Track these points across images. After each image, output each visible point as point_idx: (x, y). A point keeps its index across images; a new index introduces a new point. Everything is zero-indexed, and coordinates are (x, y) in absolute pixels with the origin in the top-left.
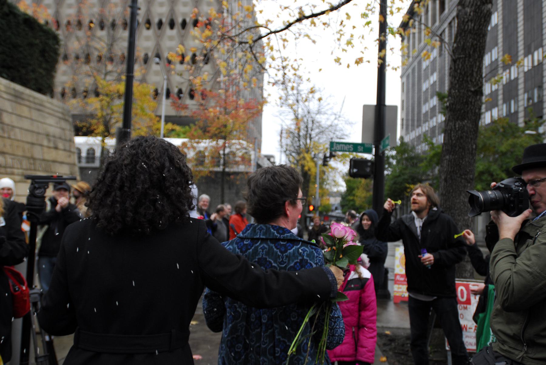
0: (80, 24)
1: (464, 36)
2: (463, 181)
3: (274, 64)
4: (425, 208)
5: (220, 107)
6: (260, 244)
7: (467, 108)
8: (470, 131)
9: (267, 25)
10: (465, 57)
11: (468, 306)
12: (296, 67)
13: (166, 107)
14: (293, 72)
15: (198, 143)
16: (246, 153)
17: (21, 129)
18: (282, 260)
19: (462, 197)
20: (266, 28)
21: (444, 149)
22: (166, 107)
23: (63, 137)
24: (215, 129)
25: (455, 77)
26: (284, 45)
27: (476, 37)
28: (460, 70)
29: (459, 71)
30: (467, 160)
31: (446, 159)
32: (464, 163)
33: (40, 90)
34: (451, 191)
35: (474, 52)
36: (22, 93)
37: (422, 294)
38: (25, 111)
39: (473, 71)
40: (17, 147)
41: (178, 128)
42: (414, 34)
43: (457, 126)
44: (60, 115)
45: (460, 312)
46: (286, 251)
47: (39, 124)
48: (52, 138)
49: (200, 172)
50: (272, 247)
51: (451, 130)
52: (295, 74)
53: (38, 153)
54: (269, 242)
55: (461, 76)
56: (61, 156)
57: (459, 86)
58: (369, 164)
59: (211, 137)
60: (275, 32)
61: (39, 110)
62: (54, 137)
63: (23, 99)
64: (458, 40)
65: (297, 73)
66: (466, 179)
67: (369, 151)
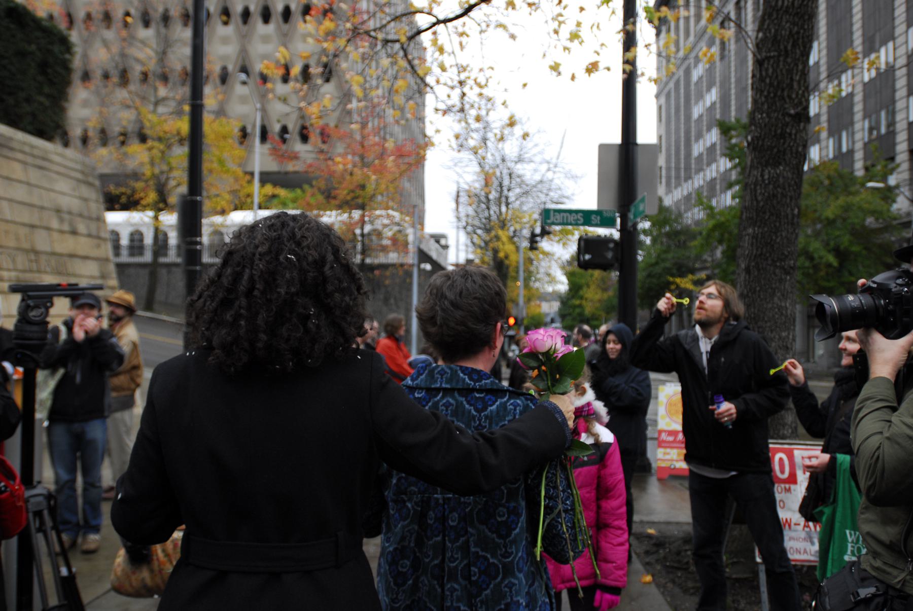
0: (107, 18)
1: (777, 18)
2: (777, 271)
3: (444, 77)
4: (718, 321)
5: (354, 154)
6: (443, 398)
7: (784, 143)
8: (789, 186)
9: (431, 9)
10: (779, 56)
11: (793, 487)
12: (483, 83)
13: (260, 158)
14: (477, 90)
16: (400, 231)
17: (10, 200)
18: (480, 424)
19: (776, 299)
20: (429, 14)
21: (744, 217)
22: (260, 158)
23: (86, 213)
24: (345, 192)
25: (762, 92)
26: (461, 44)
27: (797, 20)
28: (771, 78)
29: (768, 81)
30: (784, 234)
31: (748, 235)
32: (778, 240)
33: (41, 134)
34: (758, 289)
35: (794, 46)
36: (11, 139)
37: (711, 467)
38: (17, 170)
39: (792, 79)
40: (7, 232)
41: (282, 192)
42: (687, 19)
43: (766, 177)
44: (79, 176)
45: (778, 497)
46: (485, 409)
47: (42, 191)
48: (66, 216)
50: (462, 402)
51: (756, 184)
52: (481, 95)
53: (42, 242)
54: (456, 394)
55: (772, 89)
56: (83, 245)
57: (769, 108)
58: (612, 245)
59: (339, 207)
60: (445, 21)
61: (41, 168)
62: (70, 213)
63: (12, 149)
64: (766, 27)
65: (485, 91)
66: (782, 268)
67: (609, 223)
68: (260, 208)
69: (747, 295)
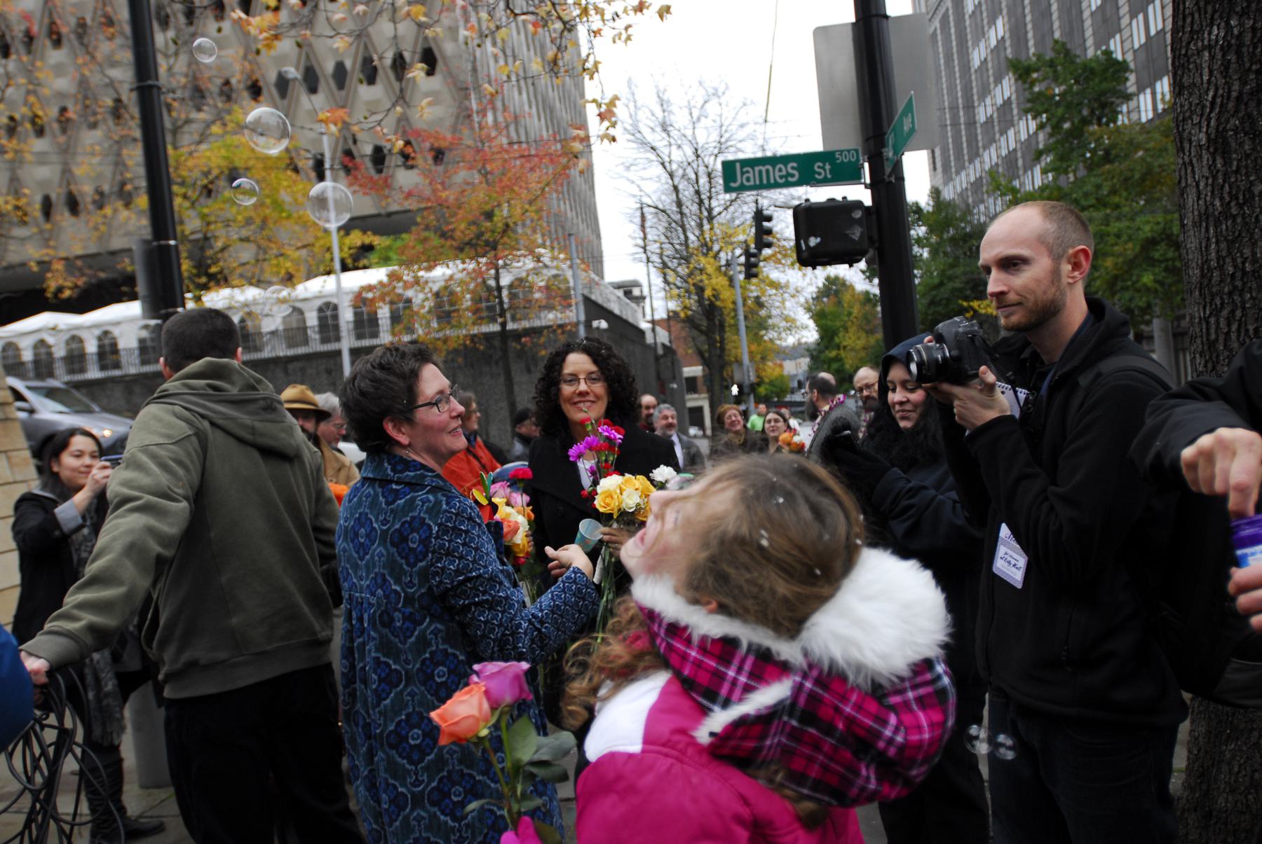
15: (429, 269)
16: (555, 276)
24: (463, 226)
41: (376, 240)
58: (858, 214)
67: (852, 176)
68: (345, 268)
69: (1226, 214)
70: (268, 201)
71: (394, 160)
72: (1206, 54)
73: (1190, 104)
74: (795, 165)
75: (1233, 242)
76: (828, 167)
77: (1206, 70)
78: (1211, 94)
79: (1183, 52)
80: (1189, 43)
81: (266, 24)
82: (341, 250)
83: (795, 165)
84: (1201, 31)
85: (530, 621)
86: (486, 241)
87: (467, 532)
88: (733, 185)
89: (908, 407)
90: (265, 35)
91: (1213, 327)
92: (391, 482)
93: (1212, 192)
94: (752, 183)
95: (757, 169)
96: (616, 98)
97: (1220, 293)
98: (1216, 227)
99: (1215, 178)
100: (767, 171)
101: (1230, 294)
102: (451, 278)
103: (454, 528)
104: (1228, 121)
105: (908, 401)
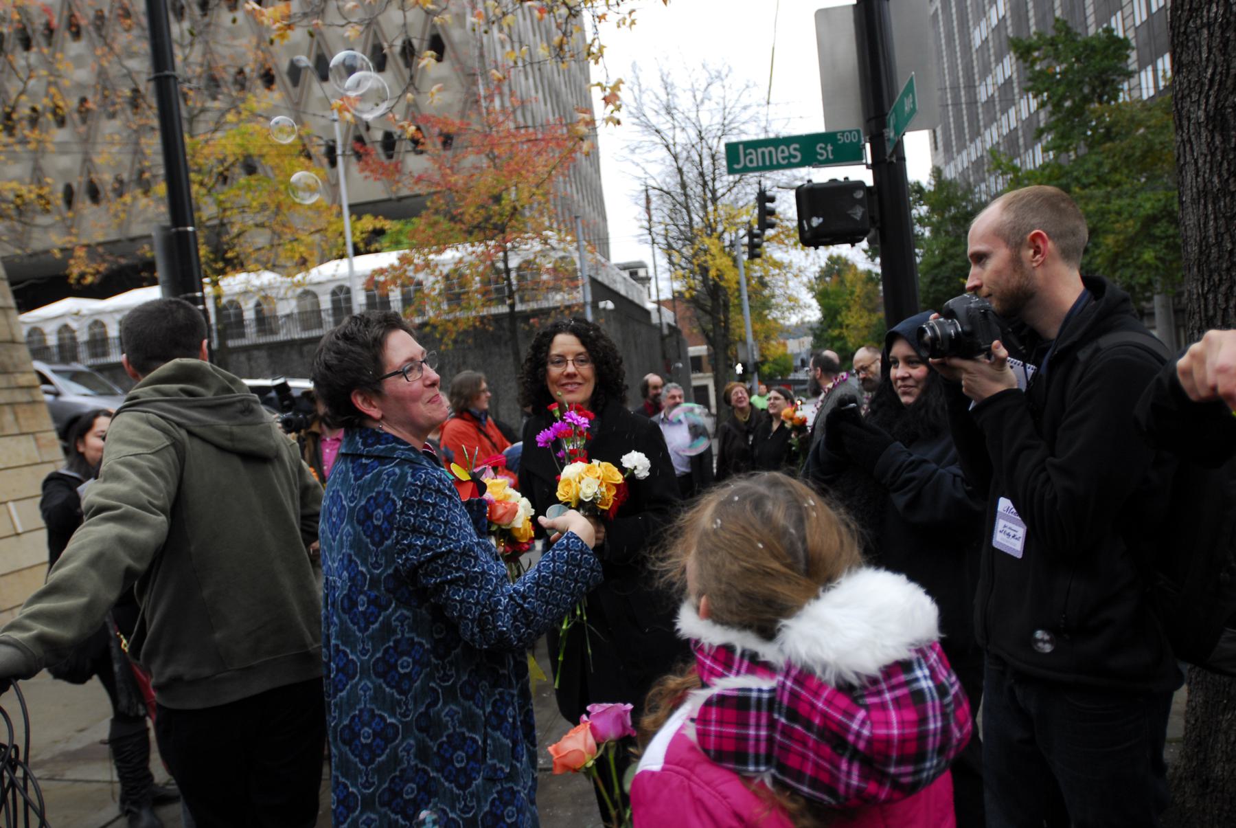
13: (356, 183)
15: (439, 252)
16: (562, 258)
22: (356, 183)
24: (472, 210)
41: (388, 225)
49: (456, 322)
58: (859, 195)
67: (853, 156)
68: (357, 252)
69: (1224, 190)
70: (282, 187)
71: (403, 146)
72: (1205, 31)
73: (1189, 81)
74: (797, 146)
75: (1232, 218)
76: (829, 148)
77: (1205, 49)
78: (1210, 71)
79: (1182, 30)
80: (1188, 21)
81: (278, 15)
82: (353, 234)
83: (797, 146)
84: (1200, 8)
85: (511, 597)
86: (495, 224)
87: (434, 505)
88: (736, 166)
89: (910, 382)
90: (278, 25)
91: (1211, 303)
92: (361, 456)
93: (1211, 169)
94: (755, 164)
95: (760, 151)
96: (620, 82)
97: (1218, 269)
98: (1214, 204)
99: (1213, 155)
100: (770, 153)
101: (1228, 270)
102: (461, 260)
103: (420, 502)
104: (1226, 99)
105: (910, 377)
